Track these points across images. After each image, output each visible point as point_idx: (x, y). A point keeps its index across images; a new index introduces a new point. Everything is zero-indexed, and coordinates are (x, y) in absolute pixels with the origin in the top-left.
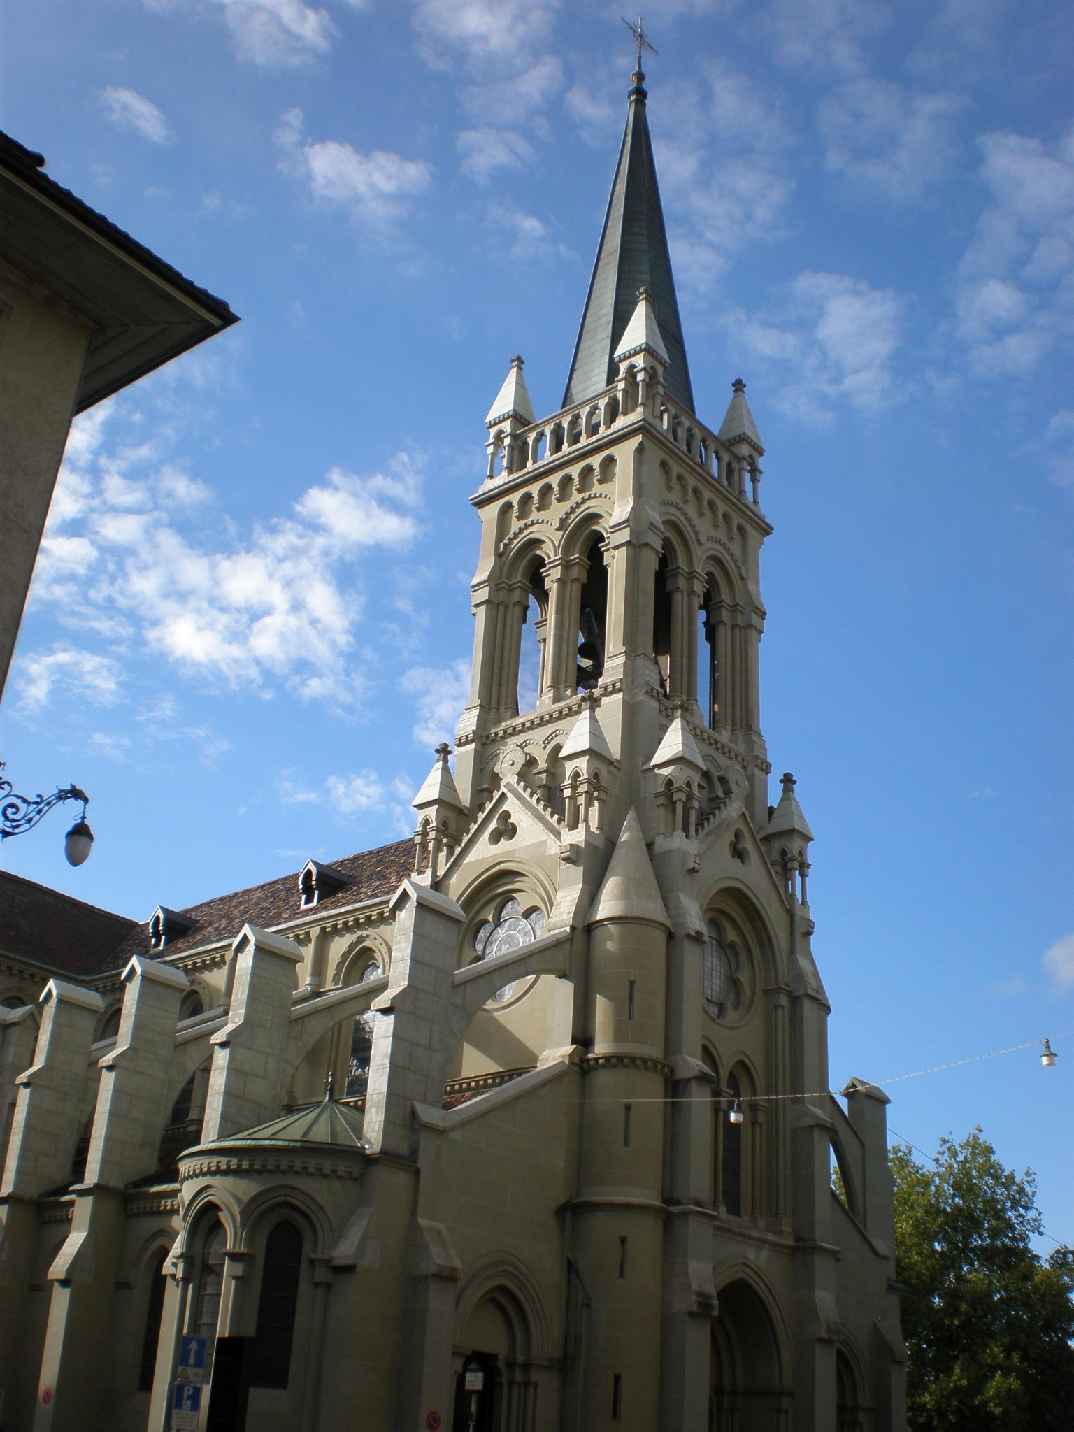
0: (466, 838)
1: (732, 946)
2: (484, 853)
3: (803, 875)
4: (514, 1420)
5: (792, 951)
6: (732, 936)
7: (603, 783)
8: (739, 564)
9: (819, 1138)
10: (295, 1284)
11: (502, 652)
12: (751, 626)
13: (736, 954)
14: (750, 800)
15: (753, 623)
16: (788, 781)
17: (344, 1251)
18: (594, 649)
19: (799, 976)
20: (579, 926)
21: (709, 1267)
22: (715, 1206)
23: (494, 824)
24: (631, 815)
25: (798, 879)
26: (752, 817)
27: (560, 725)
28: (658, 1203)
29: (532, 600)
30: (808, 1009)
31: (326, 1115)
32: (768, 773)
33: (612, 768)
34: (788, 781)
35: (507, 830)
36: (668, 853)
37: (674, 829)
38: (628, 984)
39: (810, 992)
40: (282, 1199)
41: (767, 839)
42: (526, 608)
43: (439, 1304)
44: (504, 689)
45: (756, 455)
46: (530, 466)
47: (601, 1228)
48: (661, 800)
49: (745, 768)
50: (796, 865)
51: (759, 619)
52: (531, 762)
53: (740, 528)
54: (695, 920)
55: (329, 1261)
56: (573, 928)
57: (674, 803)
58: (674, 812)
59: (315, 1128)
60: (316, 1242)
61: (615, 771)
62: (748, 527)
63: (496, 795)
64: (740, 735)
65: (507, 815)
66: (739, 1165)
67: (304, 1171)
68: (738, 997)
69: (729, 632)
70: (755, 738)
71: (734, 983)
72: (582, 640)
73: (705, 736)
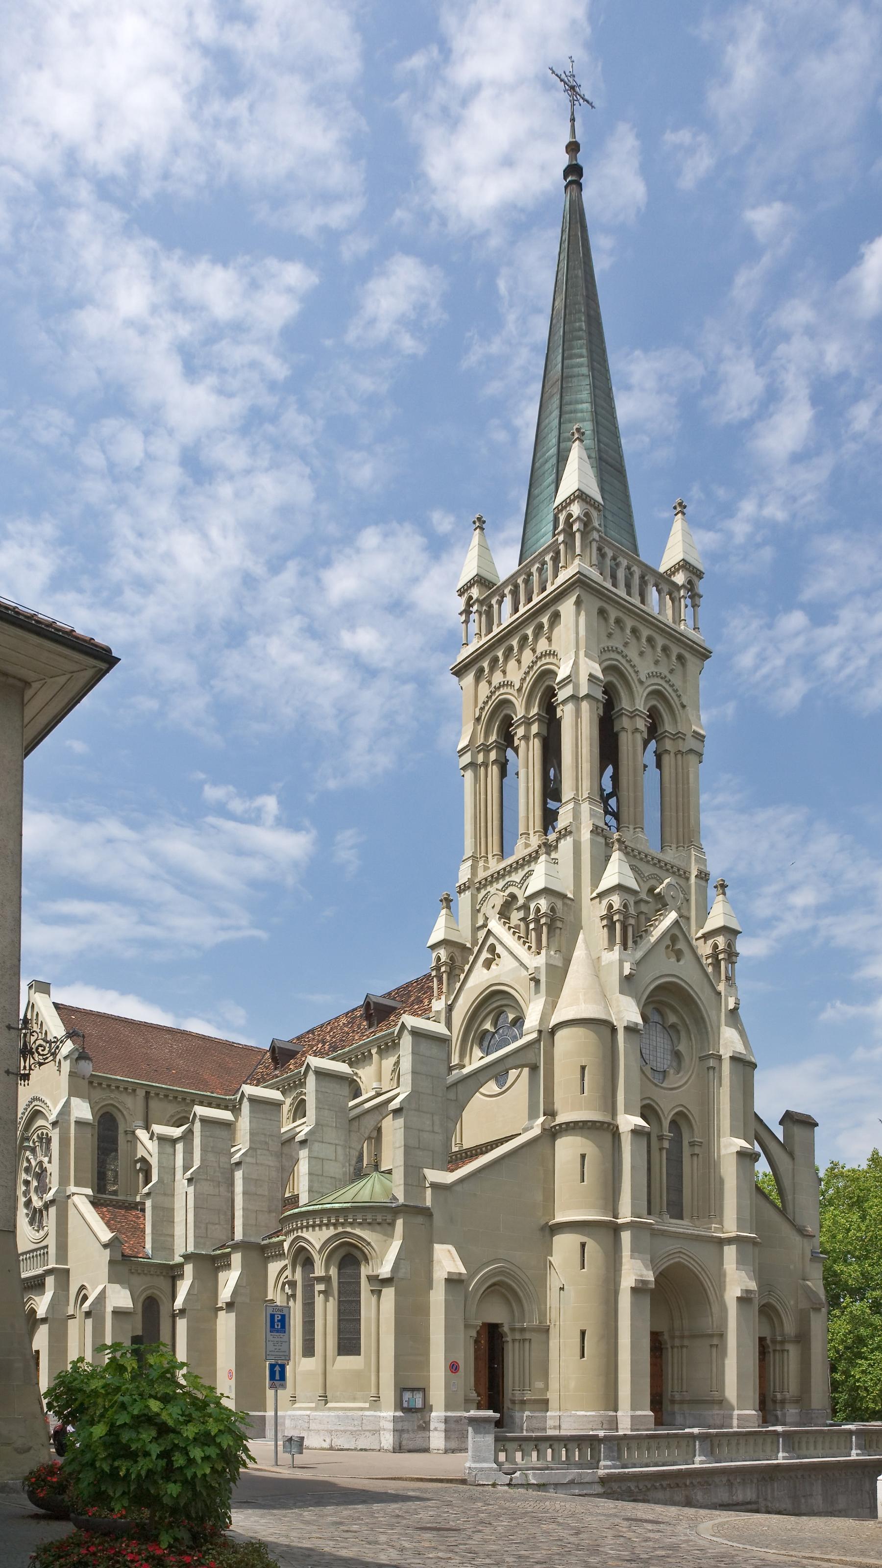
0: (467, 967)
4: (517, 1366)
8: (680, 693)
45: (695, 579)
46: (496, 630)
53: (680, 658)
61: (569, 902)
62: (687, 655)
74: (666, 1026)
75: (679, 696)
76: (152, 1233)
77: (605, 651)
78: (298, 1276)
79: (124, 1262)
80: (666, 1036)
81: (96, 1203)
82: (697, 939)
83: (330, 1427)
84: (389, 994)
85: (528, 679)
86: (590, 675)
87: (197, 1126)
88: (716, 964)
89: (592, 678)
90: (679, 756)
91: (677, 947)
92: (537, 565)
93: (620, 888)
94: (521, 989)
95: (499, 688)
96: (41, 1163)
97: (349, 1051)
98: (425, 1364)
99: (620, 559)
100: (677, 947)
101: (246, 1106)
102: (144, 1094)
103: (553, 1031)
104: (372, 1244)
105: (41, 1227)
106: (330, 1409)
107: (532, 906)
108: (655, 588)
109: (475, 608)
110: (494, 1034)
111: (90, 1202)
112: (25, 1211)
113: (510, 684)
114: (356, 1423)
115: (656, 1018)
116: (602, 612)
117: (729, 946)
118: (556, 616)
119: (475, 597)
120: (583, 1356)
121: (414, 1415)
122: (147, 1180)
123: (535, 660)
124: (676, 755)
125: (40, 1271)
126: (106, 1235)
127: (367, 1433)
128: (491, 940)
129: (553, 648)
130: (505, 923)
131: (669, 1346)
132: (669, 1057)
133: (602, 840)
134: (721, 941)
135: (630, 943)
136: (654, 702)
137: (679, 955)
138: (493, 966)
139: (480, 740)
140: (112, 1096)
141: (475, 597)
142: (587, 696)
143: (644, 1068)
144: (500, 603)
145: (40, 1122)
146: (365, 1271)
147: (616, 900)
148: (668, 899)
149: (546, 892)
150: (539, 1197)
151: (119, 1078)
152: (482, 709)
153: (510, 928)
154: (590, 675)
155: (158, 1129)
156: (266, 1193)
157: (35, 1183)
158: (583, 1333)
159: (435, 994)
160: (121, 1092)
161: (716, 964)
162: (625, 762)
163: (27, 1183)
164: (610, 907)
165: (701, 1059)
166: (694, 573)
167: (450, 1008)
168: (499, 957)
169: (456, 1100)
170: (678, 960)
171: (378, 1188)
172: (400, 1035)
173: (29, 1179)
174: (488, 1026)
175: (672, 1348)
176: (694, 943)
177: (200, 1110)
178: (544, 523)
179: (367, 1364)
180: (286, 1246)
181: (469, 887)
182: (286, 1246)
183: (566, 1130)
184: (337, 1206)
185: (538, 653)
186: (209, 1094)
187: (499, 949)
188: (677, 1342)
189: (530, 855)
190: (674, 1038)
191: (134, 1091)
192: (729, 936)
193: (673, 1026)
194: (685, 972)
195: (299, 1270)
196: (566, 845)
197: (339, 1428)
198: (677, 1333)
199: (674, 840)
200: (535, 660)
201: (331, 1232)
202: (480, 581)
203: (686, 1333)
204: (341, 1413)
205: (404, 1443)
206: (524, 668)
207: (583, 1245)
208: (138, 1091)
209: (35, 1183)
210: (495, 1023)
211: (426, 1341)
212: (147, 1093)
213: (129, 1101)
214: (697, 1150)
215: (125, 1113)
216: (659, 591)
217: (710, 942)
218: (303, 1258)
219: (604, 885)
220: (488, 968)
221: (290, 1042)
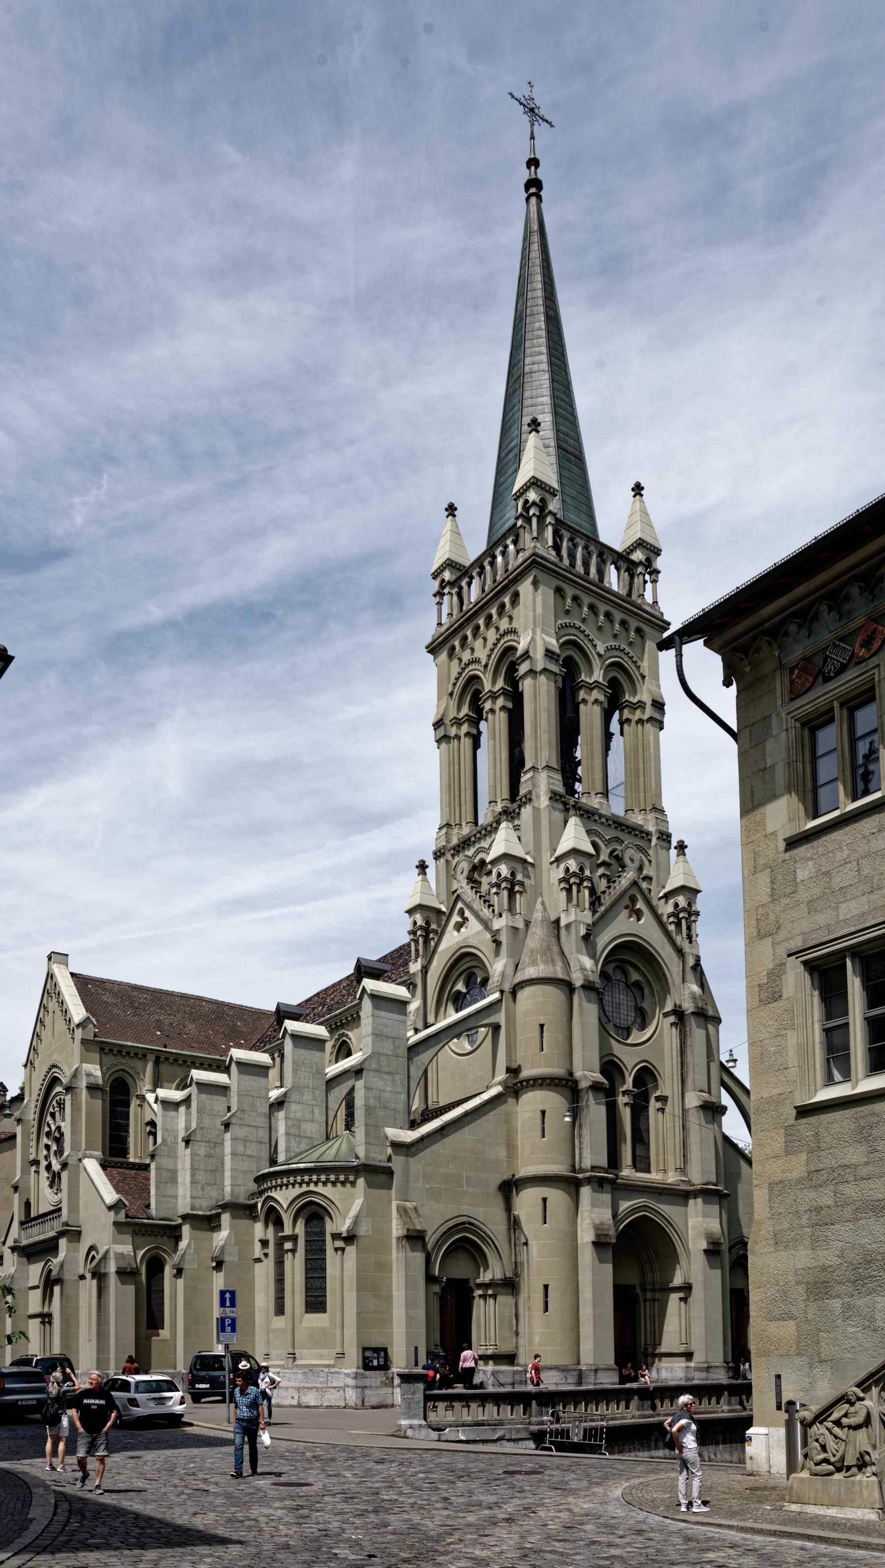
10: (324, 1251)
23: (456, 918)
38: (538, 1028)
45: (652, 555)
65: (461, 913)
74: (629, 983)
75: (638, 667)
76: (156, 1194)
77: (562, 627)
78: (270, 1235)
79: (132, 1223)
80: (630, 993)
81: (104, 1166)
82: (660, 899)
83: (297, 1384)
84: (385, 957)
85: (493, 656)
86: (547, 650)
87: (193, 1089)
88: (678, 925)
89: (549, 654)
92: (500, 548)
93: (574, 852)
94: (485, 950)
95: (468, 665)
96: (59, 1128)
97: (340, 1014)
98: (386, 1321)
99: (578, 540)
101: (234, 1068)
102: (154, 1059)
104: (336, 1202)
105: (59, 1190)
106: (297, 1366)
108: (613, 566)
109: (446, 591)
110: (465, 994)
112: (46, 1175)
113: (477, 661)
115: (619, 976)
116: (559, 591)
117: (689, 905)
118: (516, 595)
119: (447, 579)
120: (546, 1310)
123: (499, 637)
125: (52, 1234)
126: (110, 1195)
127: (333, 1390)
128: (460, 905)
129: (514, 625)
130: (472, 888)
131: (641, 1299)
132: (633, 1014)
133: (561, 806)
134: (682, 901)
136: (614, 674)
137: (639, 914)
138: (463, 930)
139: (452, 714)
140: (123, 1061)
141: (447, 579)
142: (545, 670)
143: (606, 1025)
144: (469, 584)
145: (58, 1089)
146: (330, 1227)
147: (572, 864)
148: (627, 861)
149: (505, 857)
150: (502, 1153)
151: (129, 1044)
152: (455, 684)
154: (547, 650)
155: (162, 1093)
156: (255, 1154)
157: (54, 1147)
158: (546, 1287)
159: (413, 957)
160: (132, 1058)
161: (678, 925)
163: (48, 1147)
164: (567, 870)
166: (651, 551)
167: (425, 970)
170: (639, 920)
171: (344, 1147)
172: (361, 998)
173: (50, 1143)
174: (460, 987)
175: (645, 1300)
176: (654, 902)
177: (198, 1074)
178: (508, 508)
179: (333, 1322)
180: (259, 1205)
182: (259, 1205)
183: (533, 1086)
184: (302, 1166)
185: (501, 631)
186: (218, 1057)
187: (467, 914)
188: (649, 1295)
191: (144, 1056)
192: (689, 895)
193: (637, 984)
194: (646, 929)
195: (271, 1228)
196: (526, 812)
197: (306, 1385)
198: (648, 1287)
200: (499, 637)
201: (297, 1191)
202: (449, 564)
203: (657, 1286)
206: (490, 645)
207: (545, 1200)
208: (149, 1056)
209: (54, 1147)
210: (467, 984)
211: (388, 1299)
213: (139, 1064)
216: (618, 569)
217: (671, 902)
218: (273, 1217)
219: (561, 849)
220: (458, 931)
221: (299, 1005)
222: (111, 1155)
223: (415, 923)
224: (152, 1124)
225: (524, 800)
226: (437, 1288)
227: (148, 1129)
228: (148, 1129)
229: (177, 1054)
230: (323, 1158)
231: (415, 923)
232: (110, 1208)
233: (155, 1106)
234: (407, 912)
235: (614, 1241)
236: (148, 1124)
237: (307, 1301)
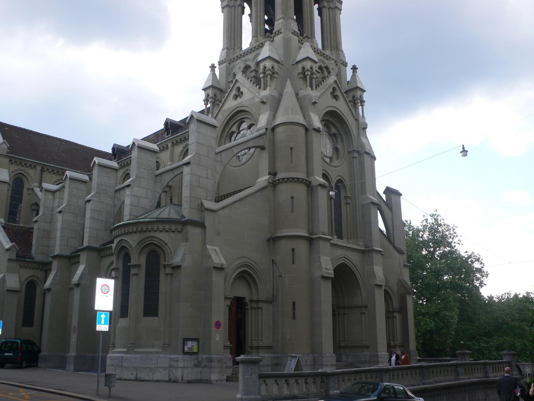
0: (223, 100)
1: (334, 135)
2: (231, 104)
3: (362, 106)
5: (359, 135)
6: (334, 131)
7: (276, 69)
9: (373, 208)
11: (234, 26)
12: (336, 7)
13: (336, 138)
14: (339, 75)
15: (337, 6)
16: (354, 68)
17: (176, 260)
18: (271, 22)
19: (362, 145)
20: (269, 127)
21: (330, 259)
22: (332, 235)
24: (289, 82)
25: (360, 107)
26: (341, 83)
27: (258, 51)
28: (307, 235)
29: (246, 5)
30: (366, 158)
31: (168, 208)
32: (346, 66)
33: (279, 65)
34: (354, 68)
35: (239, 94)
36: (304, 96)
37: (307, 87)
39: (367, 151)
40: (150, 242)
41: (347, 92)
42: (243, 8)
43: (217, 279)
44: (236, 41)
47: (284, 246)
48: (301, 76)
49: (337, 65)
50: (359, 101)
51: (340, 5)
52: (247, 67)
54: (317, 123)
55: (171, 265)
56: (266, 129)
57: (305, 76)
58: (306, 81)
59: (163, 213)
60: (165, 258)
61: (281, 66)
63: (234, 81)
64: (334, 52)
65: (239, 89)
66: (341, 220)
67: (158, 230)
68: (338, 155)
69: (327, 11)
70: (340, 52)
71: (336, 150)
72: (266, 18)
73: (319, 52)
90: (331, 10)
91: (335, 94)
100: (335, 94)
103: (273, 129)
107: (262, 65)
111: (3, 226)
114: (153, 362)
121: (192, 356)
122: (37, 214)
124: (329, 9)
135: (314, 87)
138: (238, 99)
140: (22, 168)
153: (248, 78)
160: (27, 167)
162: (306, 7)
165: (349, 152)
168: (242, 93)
169: (221, 161)
181: (225, 62)
189: (259, 46)
190: (334, 141)
191: (35, 166)
199: (329, 47)
204: (143, 355)
205: (184, 376)
212: (42, 168)
213: (31, 172)
214: (349, 201)
215: (29, 178)
222: (9, 221)
223: (208, 95)
224: (37, 205)
225: (277, 33)
226: (229, 303)
227: (33, 207)
228: (33, 207)
229: (54, 167)
230: (160, 216)
231: (208, 95)
232: (8, 250)
233: (39, 194)
234: (203, 90)
235: (333, 276)
236: (32, 205)
237: (145, 308)
